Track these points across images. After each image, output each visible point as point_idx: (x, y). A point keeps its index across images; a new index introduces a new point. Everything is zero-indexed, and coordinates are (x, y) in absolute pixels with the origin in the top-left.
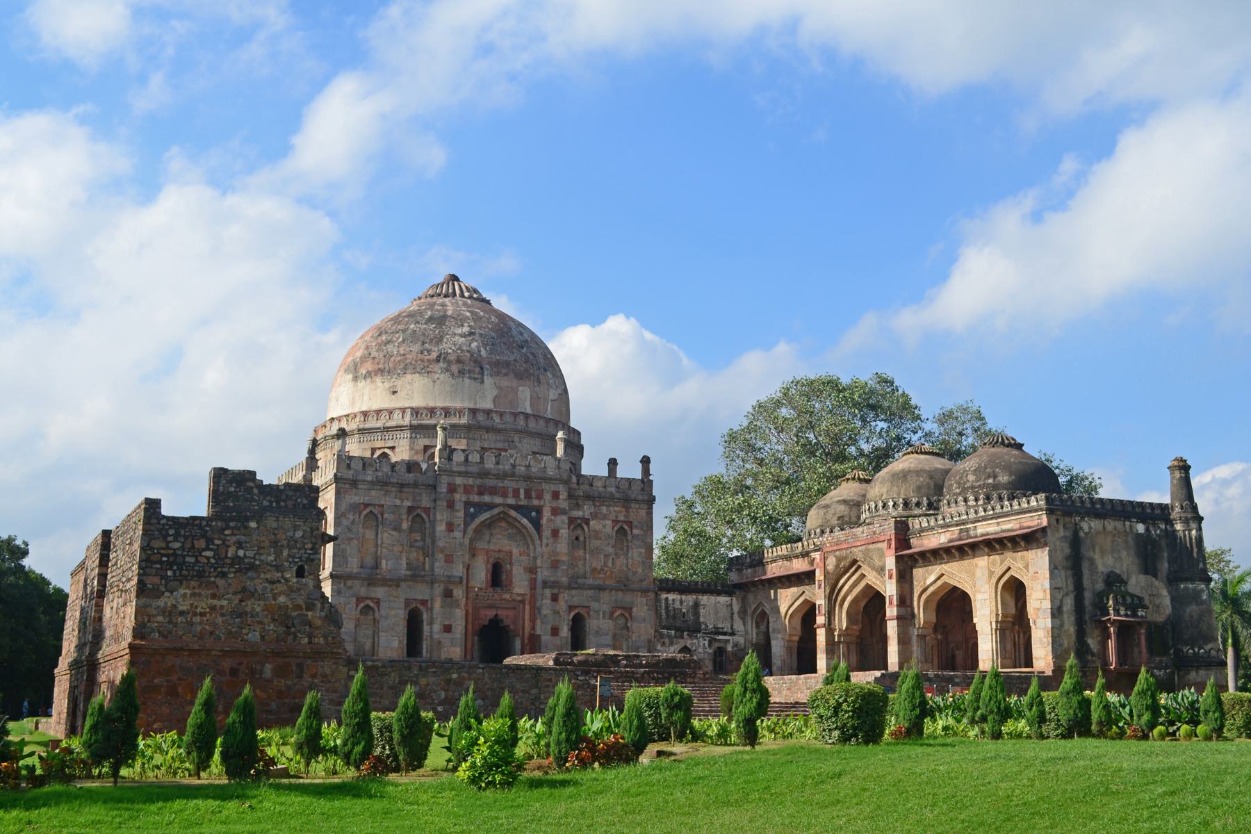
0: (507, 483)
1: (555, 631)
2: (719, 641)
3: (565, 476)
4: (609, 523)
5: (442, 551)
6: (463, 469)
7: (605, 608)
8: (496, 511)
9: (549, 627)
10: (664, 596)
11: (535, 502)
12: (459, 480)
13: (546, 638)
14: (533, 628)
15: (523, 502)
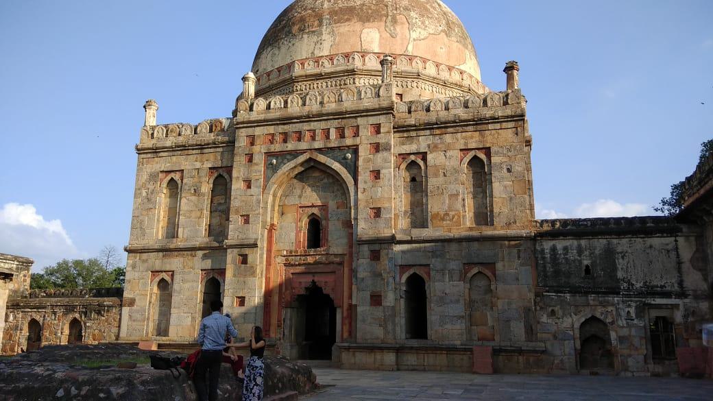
0: (313, 125)
1: (376, 300)
2: (659, 306)
3: (385, 104)
4: (456, 154)
5: (237, 212)
6: (262, 117)
7: (454, 265)
8: (302, 158)
9: (367, 295)
10: (547, 245)
11: (349, 141)
12: (258, 131)
13: (363, 309)
14: (350, 297)
15: (334, 141)
